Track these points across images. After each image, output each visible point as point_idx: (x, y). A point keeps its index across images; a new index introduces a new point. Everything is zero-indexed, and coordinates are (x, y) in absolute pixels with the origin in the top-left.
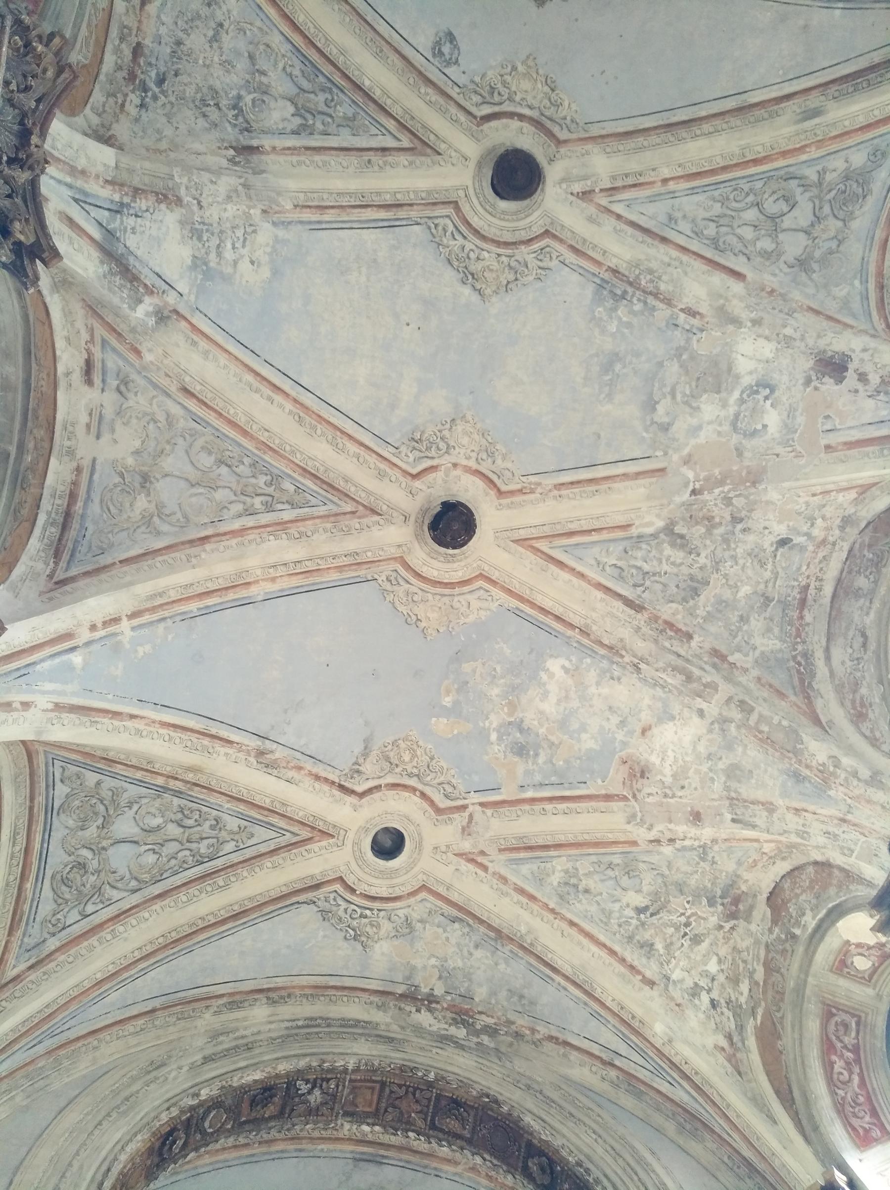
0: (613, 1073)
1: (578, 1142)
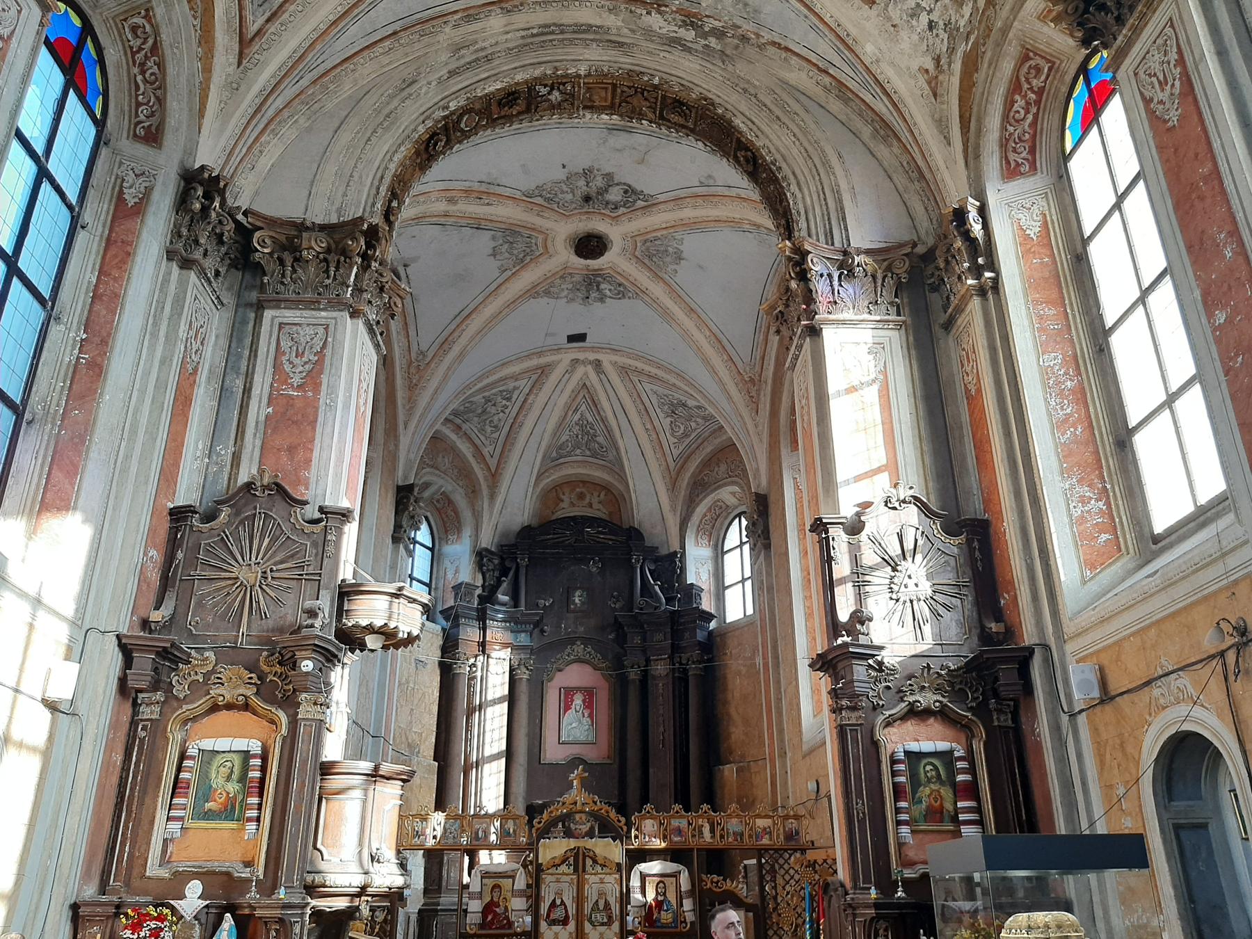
0: (827, 80)
1: (778, 143)
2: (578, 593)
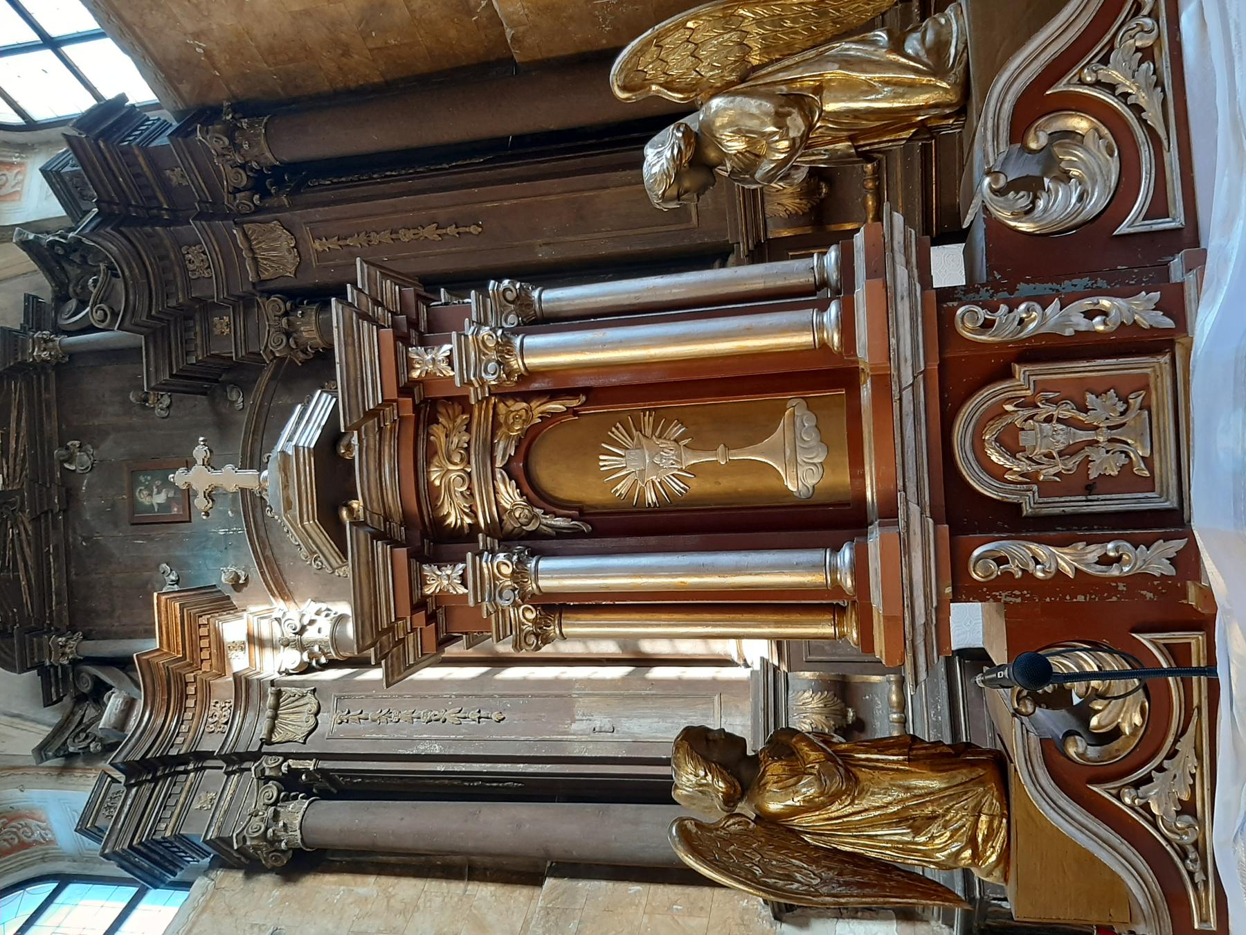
2: (143, 498)
